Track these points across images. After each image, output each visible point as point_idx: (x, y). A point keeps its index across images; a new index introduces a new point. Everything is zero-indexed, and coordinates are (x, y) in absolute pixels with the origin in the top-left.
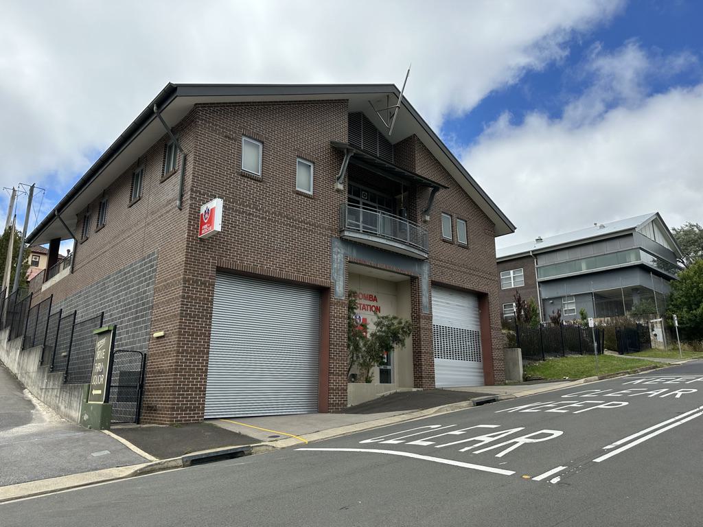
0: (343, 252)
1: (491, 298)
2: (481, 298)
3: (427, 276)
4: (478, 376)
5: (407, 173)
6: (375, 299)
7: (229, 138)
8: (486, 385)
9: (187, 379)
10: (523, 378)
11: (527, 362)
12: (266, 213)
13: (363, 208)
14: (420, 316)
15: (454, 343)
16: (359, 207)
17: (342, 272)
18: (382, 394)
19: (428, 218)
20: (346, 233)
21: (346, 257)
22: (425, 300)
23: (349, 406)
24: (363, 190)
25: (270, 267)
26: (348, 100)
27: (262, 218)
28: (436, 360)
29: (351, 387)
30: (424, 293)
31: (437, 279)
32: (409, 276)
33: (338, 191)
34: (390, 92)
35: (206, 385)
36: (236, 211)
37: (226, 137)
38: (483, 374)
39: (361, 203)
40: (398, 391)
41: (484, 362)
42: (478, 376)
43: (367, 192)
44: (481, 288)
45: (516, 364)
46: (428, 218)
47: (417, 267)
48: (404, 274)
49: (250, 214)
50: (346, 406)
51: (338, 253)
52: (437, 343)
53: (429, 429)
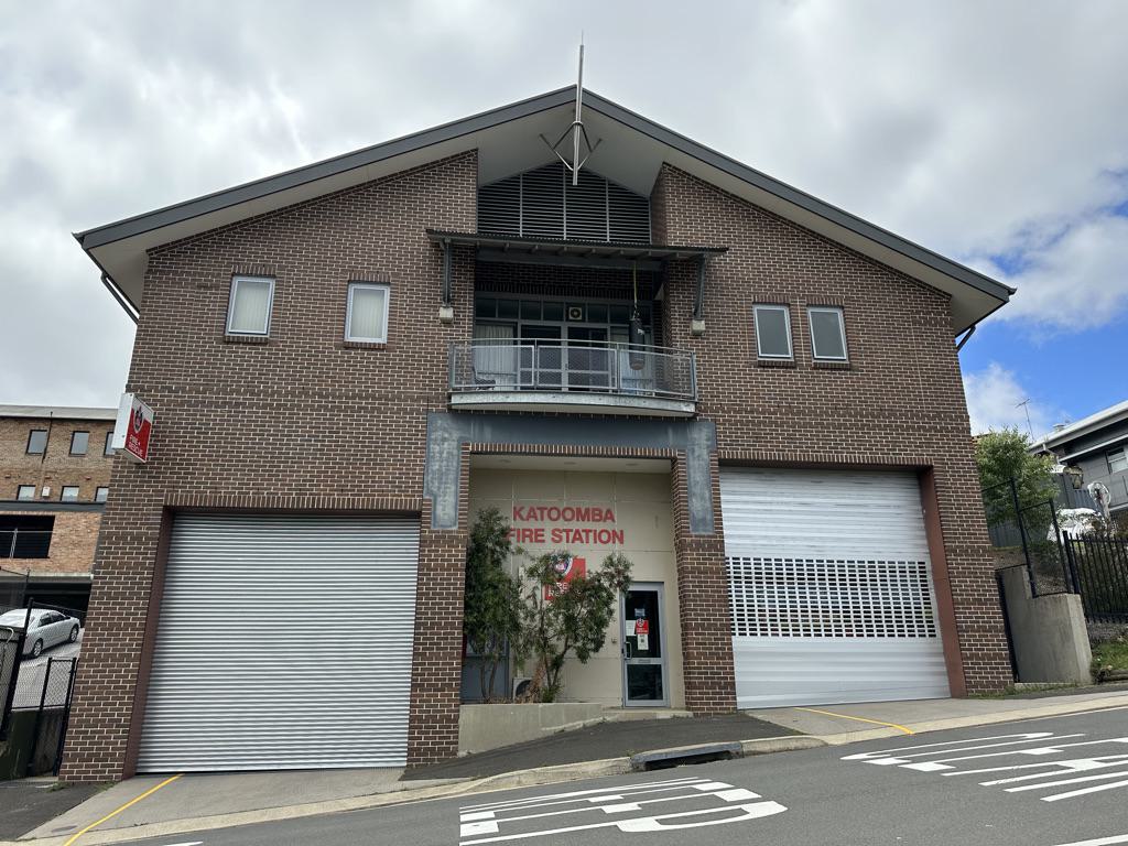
0: (456, 435)
1: (938, 477)
2: (920, 476)
3: (705, 452)
4: (940, 674)
5: (594, 249)
6: (610, 516)
7: (206, 287)
8: (953, 697)
9: (94, 704)
10: (1093, 672)
11: (1109, 630)
12: (272, 395)
13: (570, 344)
14: (700, 550)
15: (832, 598)
16: (559, 343)
17: (452, 477)
18: (561, 727)
19: (699, 326)
20: (455, 400)
21: (463, 444)
22: (698, 506)
23: (462, 754)
24: (569, 305)
25: (280, 493)
26: (476, 150)
27: (264, 407)
28: (737, 640)
29: (470, 715)
30: (697, 490)
31: (727, 454)
32: (666, 458)
33: (446, 322)
34: (563, 99)
35: (411, 706)
36: (211, 403)
37: (199, 287)
38: (944, 669)
39: (564, 332)
40: (609, 719)
41: (944, 637)
42: (940, 674)
43: (582, 305)
44: (923, 457)
45: (1067, 636)
46: (699, 326)
47: (670, 432)
48: (657, 458)
49: (237, 405)
50: (454, 753)
51: (444, 440)
52: (907, 595)
53: (661, 822)
